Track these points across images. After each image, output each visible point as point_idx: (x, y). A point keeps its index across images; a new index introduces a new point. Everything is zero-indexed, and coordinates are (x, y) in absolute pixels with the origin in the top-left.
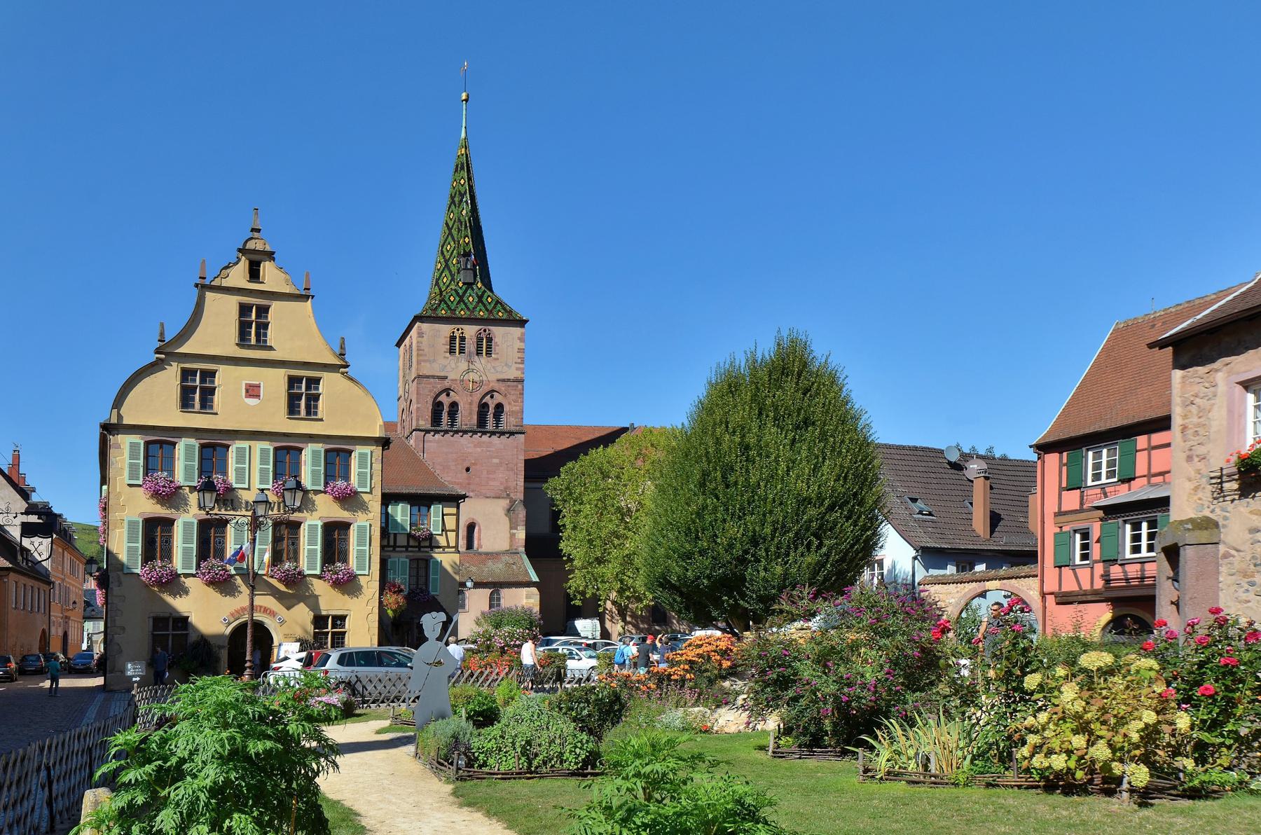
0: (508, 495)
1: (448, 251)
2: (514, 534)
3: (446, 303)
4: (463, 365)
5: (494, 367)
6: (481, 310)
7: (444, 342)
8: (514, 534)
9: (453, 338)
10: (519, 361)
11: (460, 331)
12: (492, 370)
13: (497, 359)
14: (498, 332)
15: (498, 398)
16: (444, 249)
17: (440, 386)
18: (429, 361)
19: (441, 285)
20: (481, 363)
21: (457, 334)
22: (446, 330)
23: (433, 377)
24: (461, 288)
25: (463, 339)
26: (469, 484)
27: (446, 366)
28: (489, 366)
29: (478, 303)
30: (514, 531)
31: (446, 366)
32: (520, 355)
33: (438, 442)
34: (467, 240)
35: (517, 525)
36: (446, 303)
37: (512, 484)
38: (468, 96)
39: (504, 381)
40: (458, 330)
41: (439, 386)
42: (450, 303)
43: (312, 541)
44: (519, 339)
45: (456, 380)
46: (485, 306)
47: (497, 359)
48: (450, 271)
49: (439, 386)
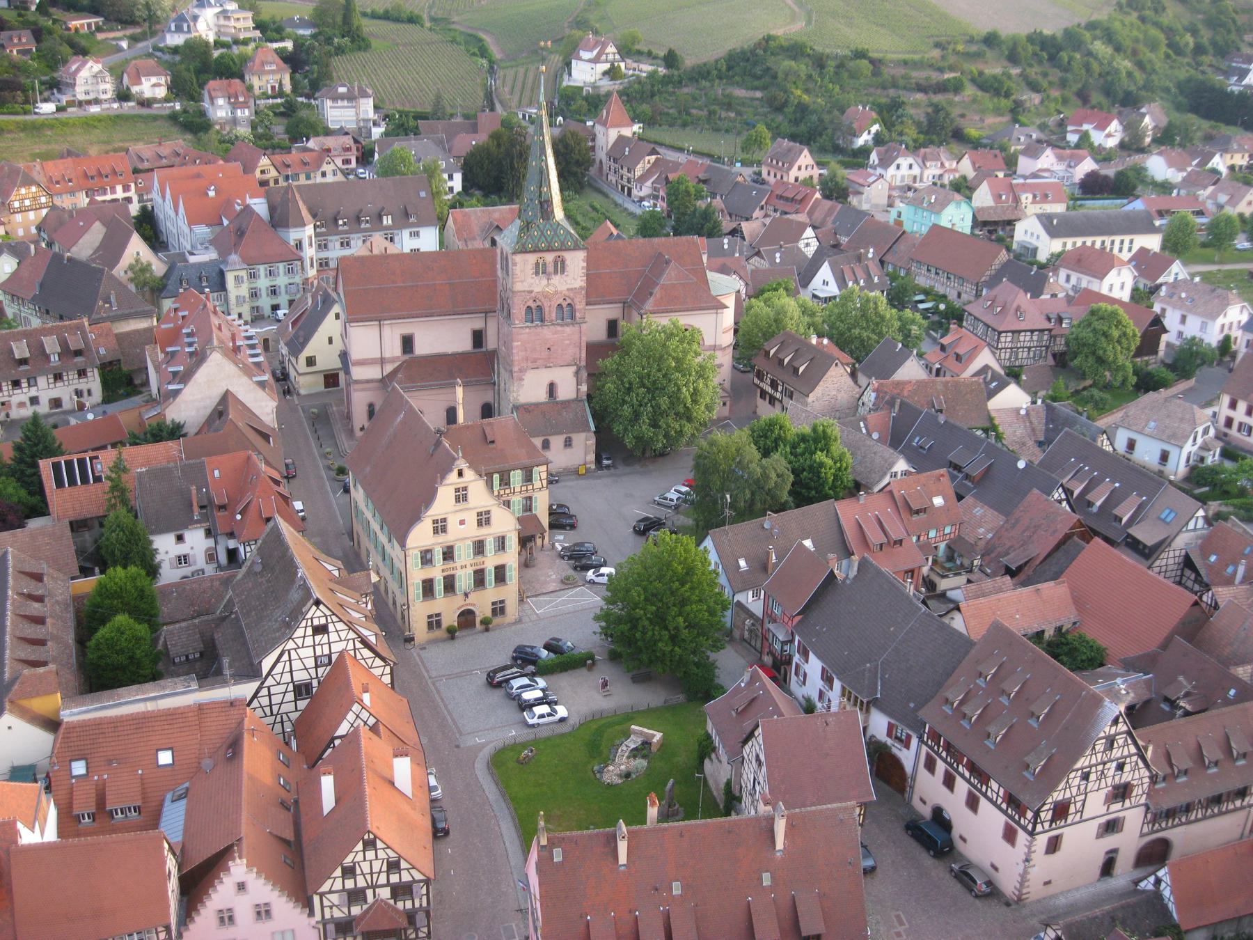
4: (544, 282)
9: (537, 264)
14: (568, 256)
15: (569, 301)
21: (541, 261)
22: (532, 258)
25: (544, 265)
39: (572, 289)
43: (490, 580)
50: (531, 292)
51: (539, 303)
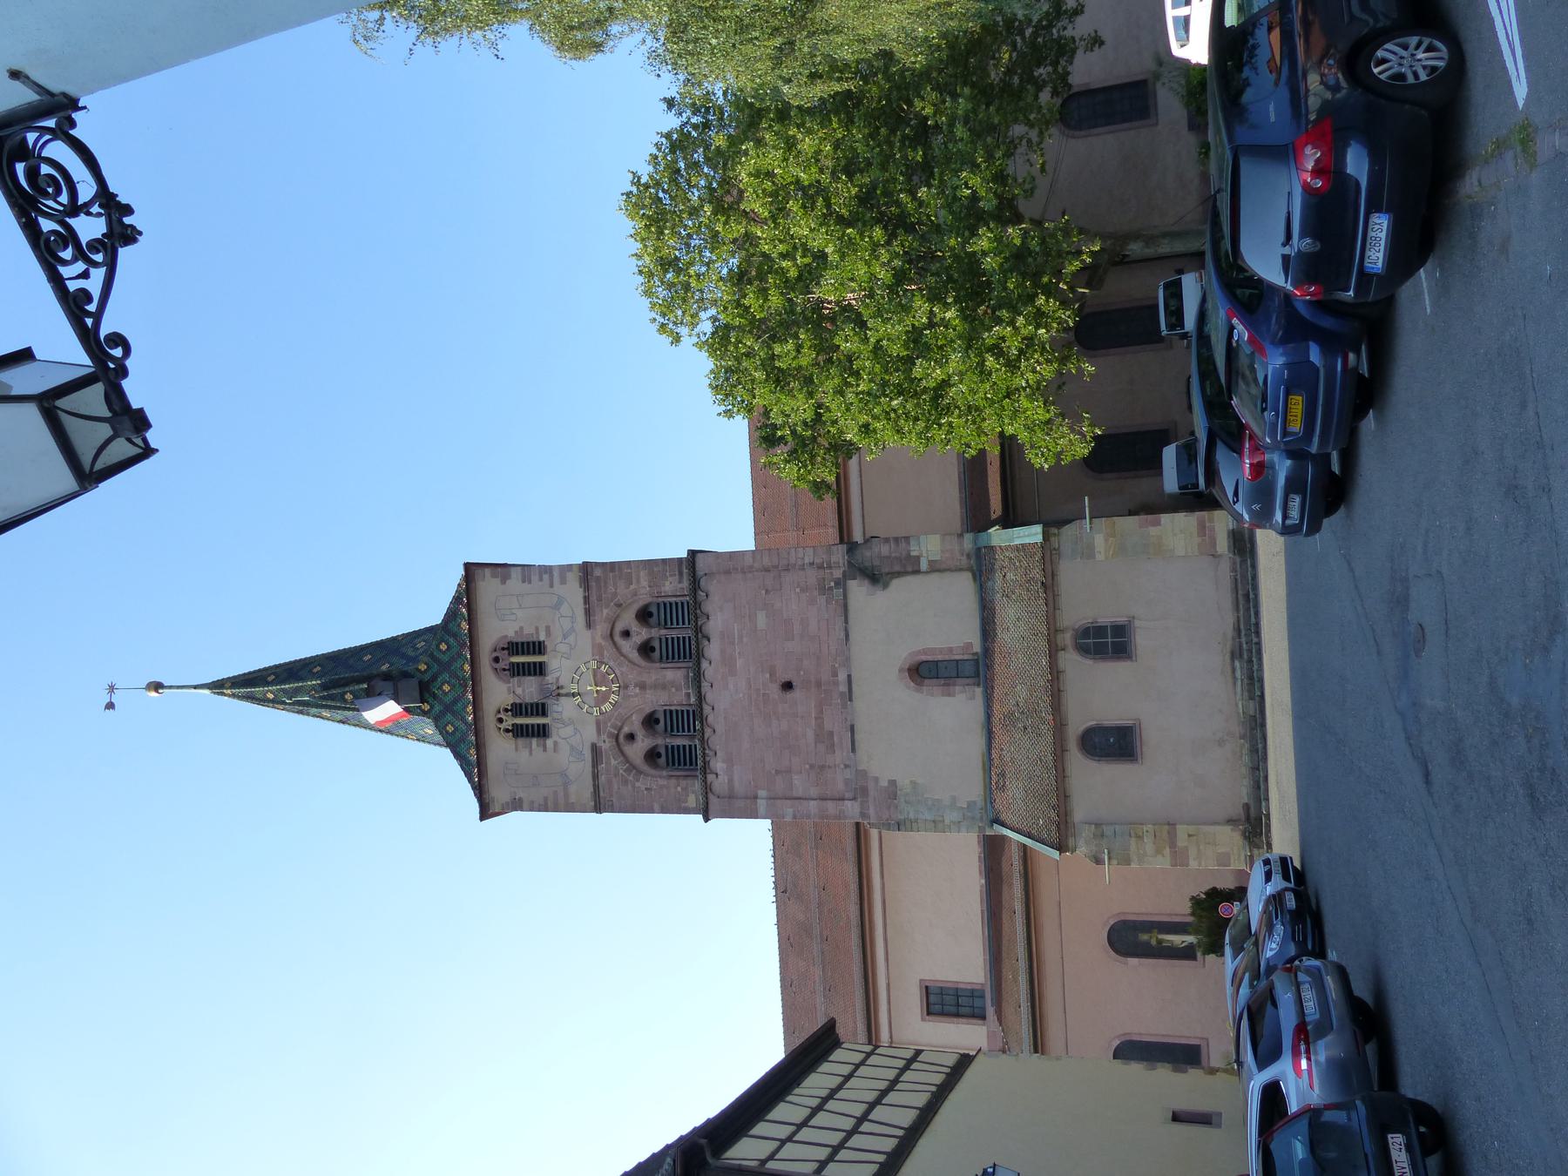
0: (838, 583)
2: (931, 563)
5: (565, 637)
7: (525, 753)
8: (931, 563)
9: (519, 732)
10: (546, 577)
11: (502, 716)
12: (571, 639)
13: (548, 629)
15: (628, 620)
17: (612, 762)
18: (566, 785)
20: (559, 666)
21: (510, 721)
23: (595, 777)
25: (517, 709)
26: (819, 684)
27: (572, 748)
28: (562, 648)
30: (924, 566)
31: (572, 748)
32: (535, 578)
33: (729, 761)
35: (909, 556)
37: (812, 576)
40: (501, 721)
41: (613, 762)
45: (598, 723)
47: (548, 629)
49: (613, 762)
50: (595, 749)
51: (635, 725)
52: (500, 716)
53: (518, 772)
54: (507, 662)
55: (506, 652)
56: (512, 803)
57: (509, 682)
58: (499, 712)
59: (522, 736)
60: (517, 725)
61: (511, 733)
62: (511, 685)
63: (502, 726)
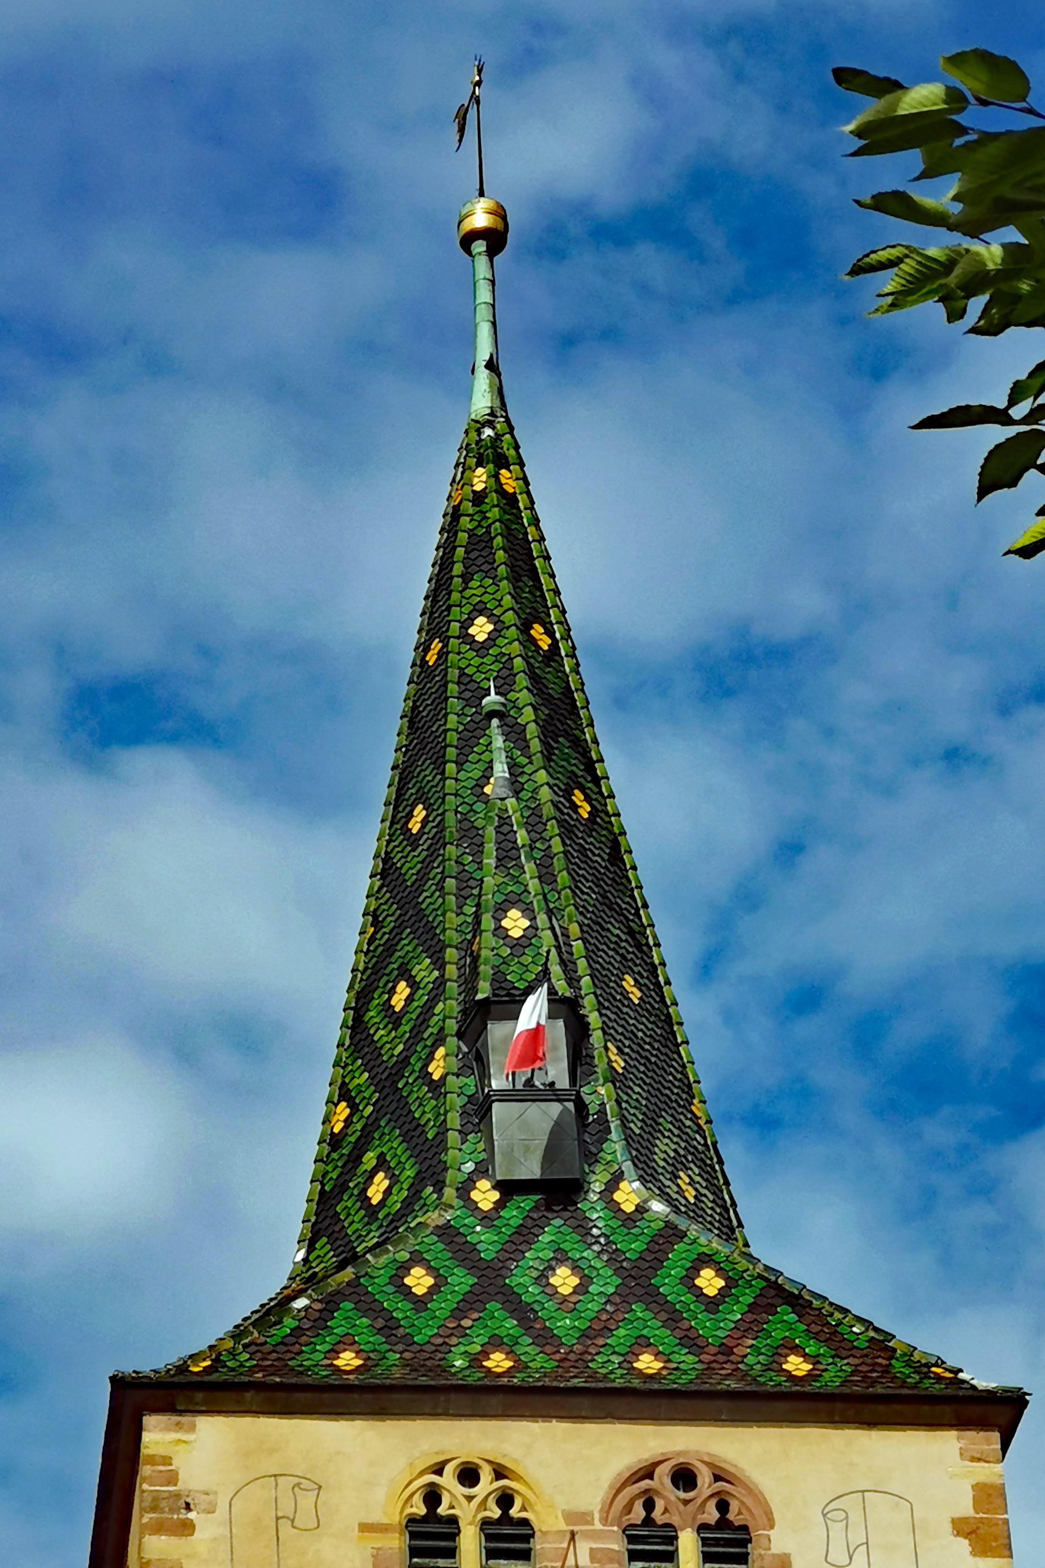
1: (395, 1019)
3: (369, 1306)
6: (642, 1343)
11: (486, 1484)
16: (372, 1015)
19: (354, 1223)
24: (487, 1219)
29: (622, 1298)
34: (515, 923)
36: (369, 1306)
38: (500, 213)
40: (469, 1476)
42: (401, 1310)
44: (962, 1528)
46: (672, 1318)
48: (412, 1131)
52: (486, 1474)
53: (285, 1526)
54: (675, 1520)
55: (712, 1515)
56: (177, 1496)
57: (605, 1521)
58: (500, 1473)
59: (414, 1552)
60: (454, 1536)
61: (422, 1510)
62: (598, 1526)
63: (448, 1480)
